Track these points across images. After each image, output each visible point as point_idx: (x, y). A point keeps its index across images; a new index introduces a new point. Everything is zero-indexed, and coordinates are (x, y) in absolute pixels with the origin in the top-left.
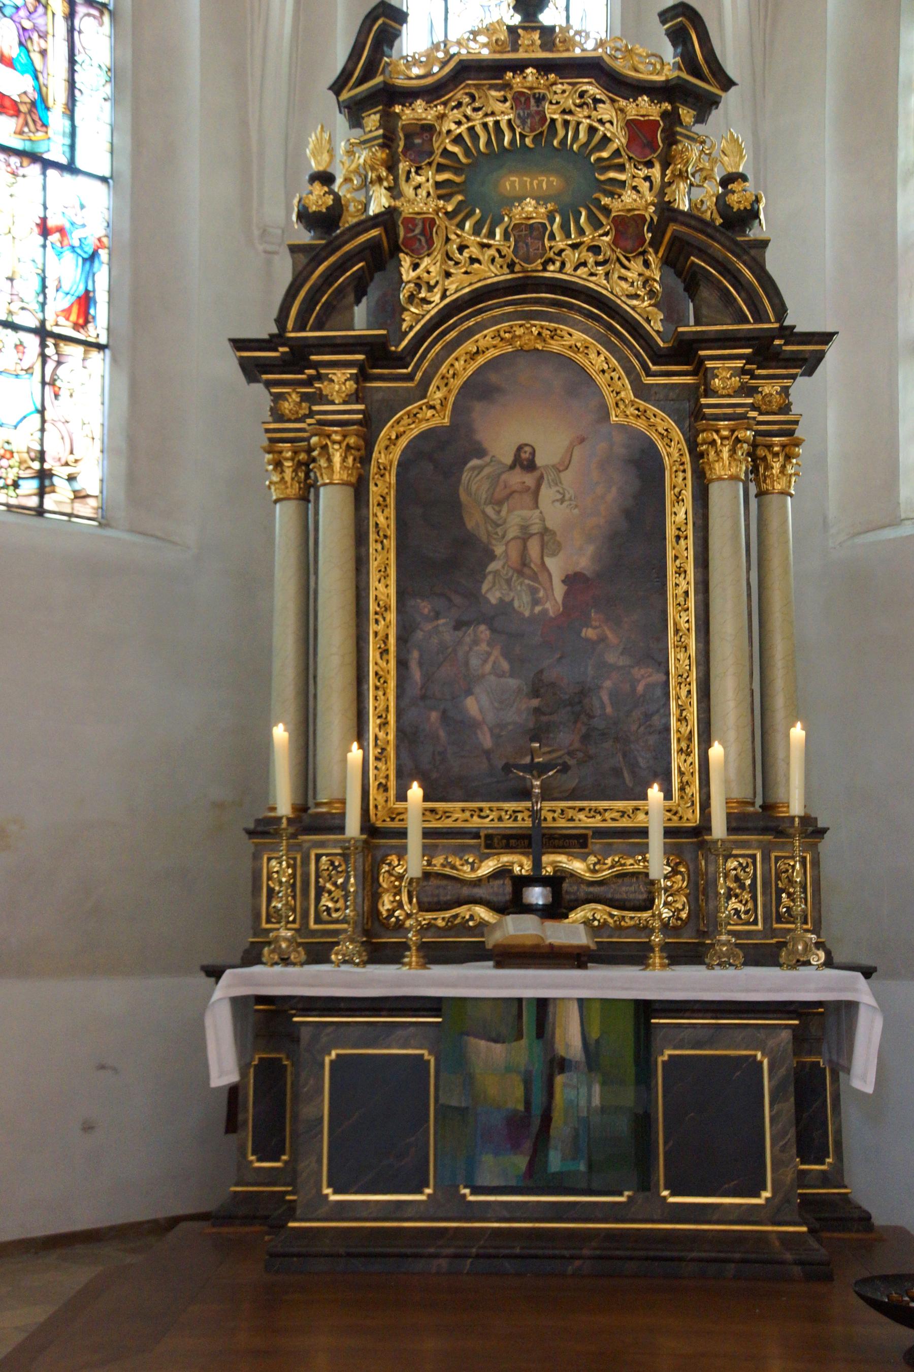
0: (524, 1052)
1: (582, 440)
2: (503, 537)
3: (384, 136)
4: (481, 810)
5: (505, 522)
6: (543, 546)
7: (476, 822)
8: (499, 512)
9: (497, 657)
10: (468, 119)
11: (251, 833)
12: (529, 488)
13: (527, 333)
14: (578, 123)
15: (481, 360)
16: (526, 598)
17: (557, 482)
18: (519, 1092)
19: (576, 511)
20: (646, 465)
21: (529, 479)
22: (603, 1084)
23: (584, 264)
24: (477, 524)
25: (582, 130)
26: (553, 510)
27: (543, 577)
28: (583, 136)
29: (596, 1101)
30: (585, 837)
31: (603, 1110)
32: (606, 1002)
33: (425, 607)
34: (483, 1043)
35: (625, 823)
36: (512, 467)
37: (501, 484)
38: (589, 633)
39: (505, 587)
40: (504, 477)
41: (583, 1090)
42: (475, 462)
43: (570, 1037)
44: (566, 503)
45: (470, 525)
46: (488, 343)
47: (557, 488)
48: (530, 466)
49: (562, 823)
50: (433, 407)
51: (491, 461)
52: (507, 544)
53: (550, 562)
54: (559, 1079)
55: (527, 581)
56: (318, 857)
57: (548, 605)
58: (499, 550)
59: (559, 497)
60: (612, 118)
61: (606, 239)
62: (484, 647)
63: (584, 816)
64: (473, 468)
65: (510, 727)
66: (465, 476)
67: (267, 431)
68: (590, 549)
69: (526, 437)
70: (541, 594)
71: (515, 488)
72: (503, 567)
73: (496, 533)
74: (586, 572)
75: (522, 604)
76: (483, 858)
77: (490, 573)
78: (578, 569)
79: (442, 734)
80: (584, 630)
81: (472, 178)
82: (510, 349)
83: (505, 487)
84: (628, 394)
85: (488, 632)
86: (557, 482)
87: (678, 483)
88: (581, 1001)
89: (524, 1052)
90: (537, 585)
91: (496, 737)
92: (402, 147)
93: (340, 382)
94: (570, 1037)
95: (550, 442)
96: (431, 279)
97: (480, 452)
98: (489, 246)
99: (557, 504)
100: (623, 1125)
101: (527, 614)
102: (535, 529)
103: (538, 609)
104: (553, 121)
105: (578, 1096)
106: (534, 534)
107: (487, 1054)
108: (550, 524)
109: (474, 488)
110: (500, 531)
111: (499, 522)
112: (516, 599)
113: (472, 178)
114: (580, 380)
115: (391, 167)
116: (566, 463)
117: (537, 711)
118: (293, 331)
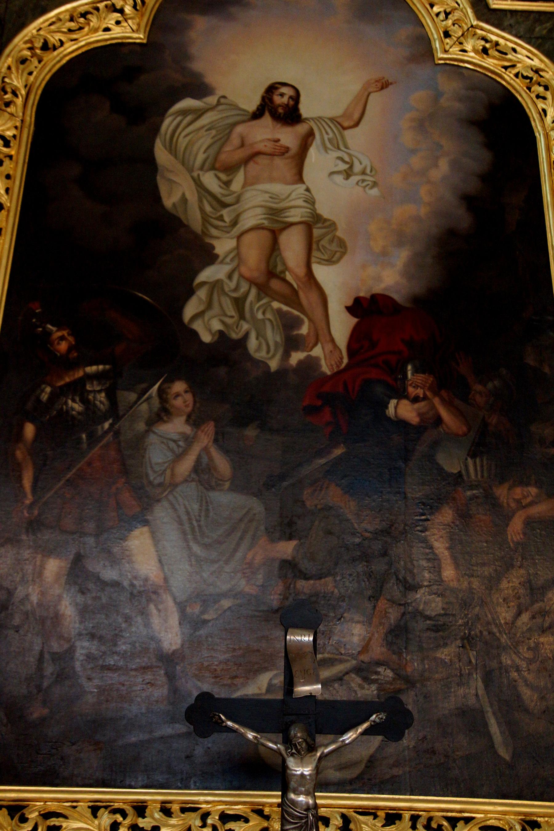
1: (384, 85)
2: (235, 223)
5: (238, 201)
6: (310, 245)
8: (227, 184)
9: (206, 449)
12: (287, 149)
16: (273, 336)
19: (375, 192)
21: (288, 137)
24: (184, 200)
26: (328, 185)
27: (308, 298)
33: (62, 338)
36: (257, 115)
37: (235, 140)
38: (402, 410)
39: (231, 311)
40: (239, 129)
42: (187, 103)
44: (354, 179)
45: (169, 200)
47: (339, 154)
48: (291, 115)
51: (219, 103)
52: (239, 237)
53: (321, 272)
55: (276, 305)
57: (317, 352)
58: (223, 246)
59: (343, 167)
62: (176, 427)
64: (184, 113)
65: (226, 603)
68: (402, 257)
69: (287, 71)
70: (304, 330)
71: (261, 147)
72: (230, 277)
73: (221, 218)
74: (396, 297)
75: (264, 348)
77: (203, 283)
78: (378, 289)
79: (68, 609)
80: (393, 403)
83: (242, 145)
85: (189, 397)
90: (296, 313)
91: (192, 623)
95: (326, 84)
97: (199, 88)
99: (339, 179)
101: (274, 365)
103: (296, 357)
106: (292, 224)
108: (323, 210)
109: (182, 143)
110: (226, 213)
111: (228, 200)
112: (253, 335)
116: (356, 116)
117: (289, 569)
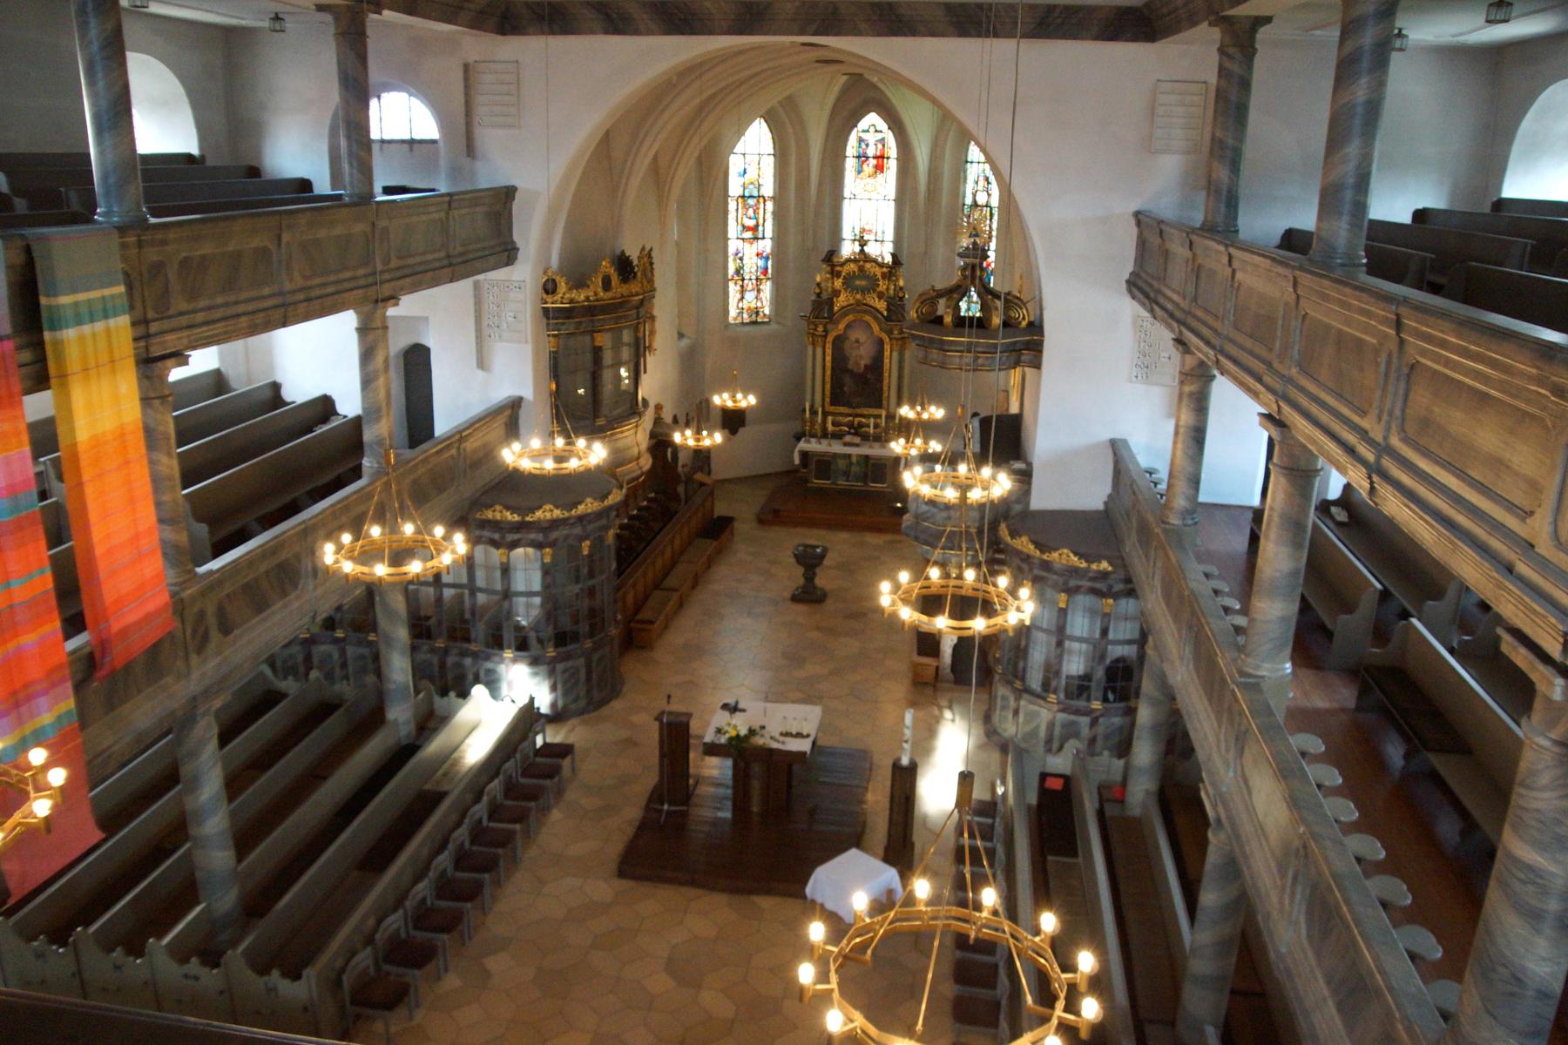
13: (859, 316)
20: (881, 342)
43: (854, 460)
46: (851, 317)
63: (865, 411)
81: (849, 281)
87: (887, 347)
92: (834, 274)
93: (820, 329)
94: (854, 460)
96: (842, 301)
105: (855, 469)
113: (849, 281)
114: (869, 326)
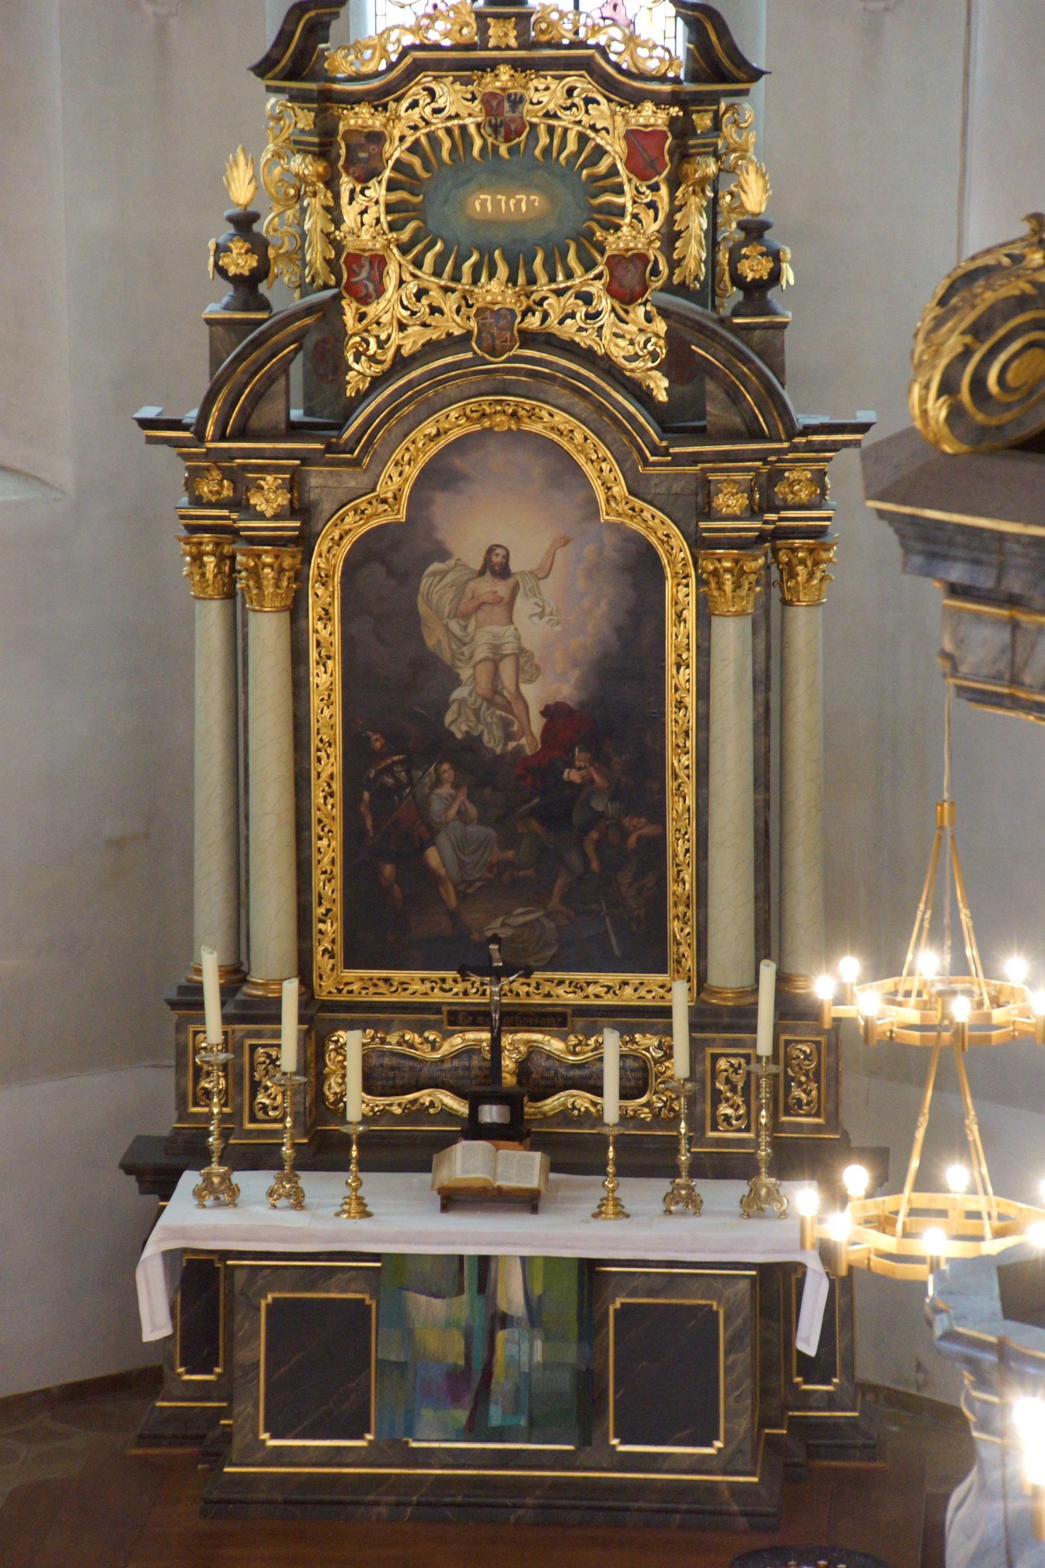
0: (463, 1307)
3: (321, 145)
4: (443, 980)
5: (472, 640)
6: (518, 670)
7: (437, 997)
10: (428, 123)
11: (174, 1005)
14: (566, 130)
15: (443, 442)
17: (535, 592)
18: (460, 1346)
19: (558, 628)
20: (642, 566)
21: (502, 588)
22: (546, 1340)
23: (572, 316)
25: (572, 136)
26: (530, 626)
28: (572, 145)
29: (538, 1357)
30: (564, 1016)
31: (545, 1366)
32: (549, 1262)
34: (423, 1299)
35: (609, 1000)
36: (482, 573)
41: (525, 1347)
42: (436, 566)
45: (430, 642)
48: (503, 572)
49: (537, 1000)
50: (384, 501)
54: (501, 1335)
56: (253, 1048)
57: (523, 741)
58: (465, 673)
60: (610, 126)
61: (599, 284)
62: (446, 790)
64: (434, 574)
66: (425, 583)
67: (183, 517)
71: (485, 598)
76: (447, 1035)
78: (559, 698)
82: (477, 427)
84: (620, 489)
86: (535, 592)
88: (524, 1260)
89: (463, 1307)
94: (512, 1294)
97: (443, 555)
98: (453, 290)
100: (565, 1381)
102: (508, 649)
103: (512, 745)
104: (534, 126)
107: (428, 1311)
108: (526, 644)
114: (565, 469)
115: (331, 182)
118: (213, 441)
